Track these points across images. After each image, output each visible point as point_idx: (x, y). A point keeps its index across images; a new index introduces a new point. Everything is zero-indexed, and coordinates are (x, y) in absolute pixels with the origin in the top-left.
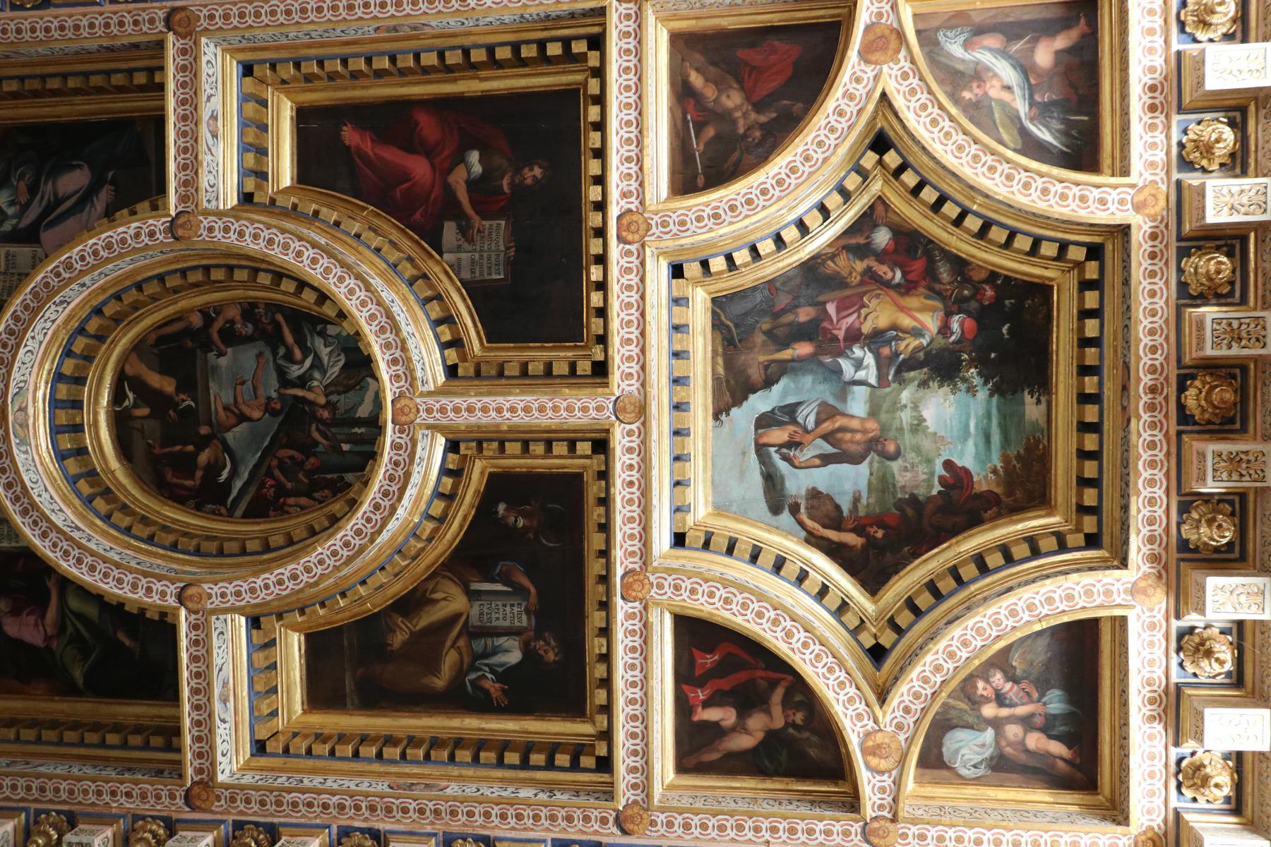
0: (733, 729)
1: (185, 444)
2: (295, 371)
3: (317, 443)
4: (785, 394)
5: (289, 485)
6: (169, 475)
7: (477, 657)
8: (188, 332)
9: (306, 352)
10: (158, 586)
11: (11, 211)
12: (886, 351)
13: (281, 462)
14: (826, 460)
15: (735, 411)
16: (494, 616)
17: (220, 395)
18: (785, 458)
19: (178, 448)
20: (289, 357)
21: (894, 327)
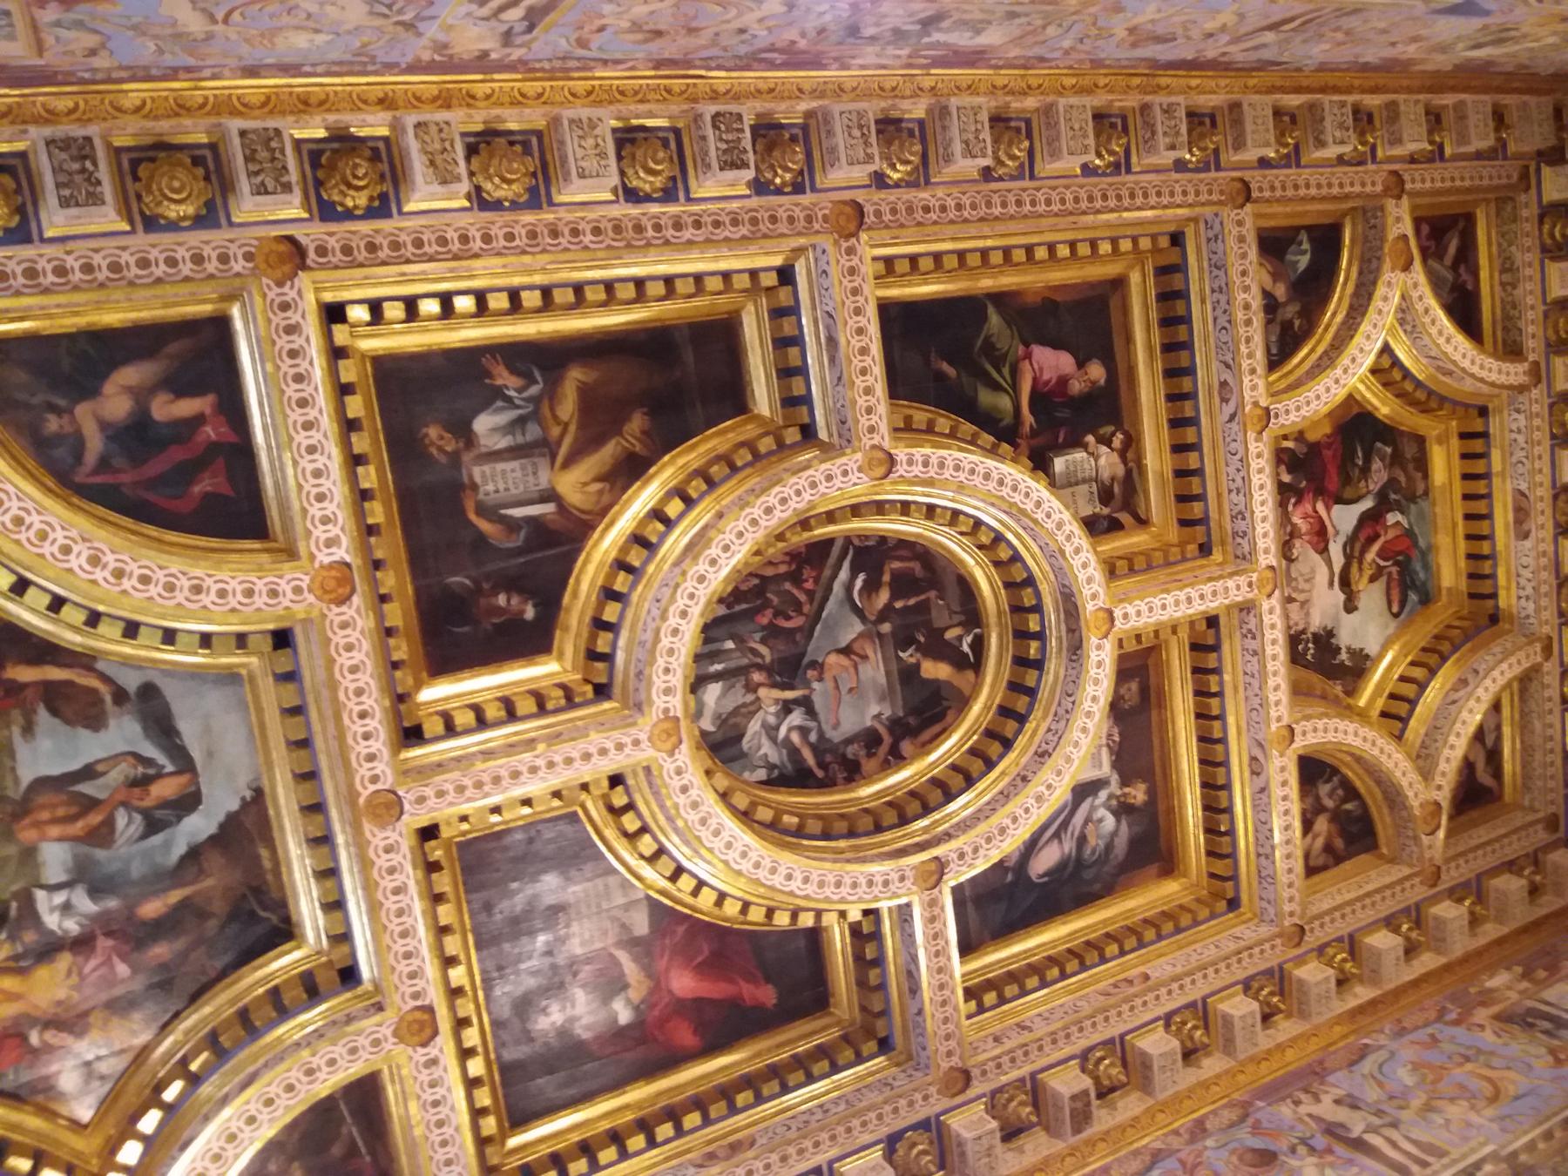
0: (153, 389)
1: (906, 608)
2: (796, 718)
3: (763, 641)
4: (167, 845)
5: (787, 586)
6: (916, 567)
7: (535, 416)
8: (913, 732)
9: (787, 741)
10: (917, 470)
11: (1102, 812)
13: (799, 610)
14: (89, 772)
16: (518, 474)
17: (875, 670)
18: (148, 762)
19: (912, 602)
20: (804, 731)
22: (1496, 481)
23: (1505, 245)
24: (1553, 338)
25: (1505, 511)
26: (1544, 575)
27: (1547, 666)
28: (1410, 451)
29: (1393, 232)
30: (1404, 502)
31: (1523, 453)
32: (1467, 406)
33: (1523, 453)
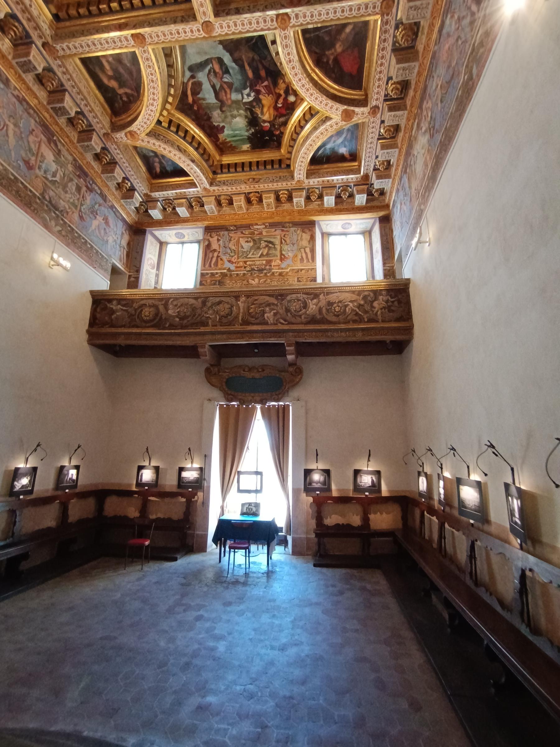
4: (233, 68)
12: (255, 104)
14: (213, 87)
15: (221, 47)
18: (210, 71)
21: (263, 106)
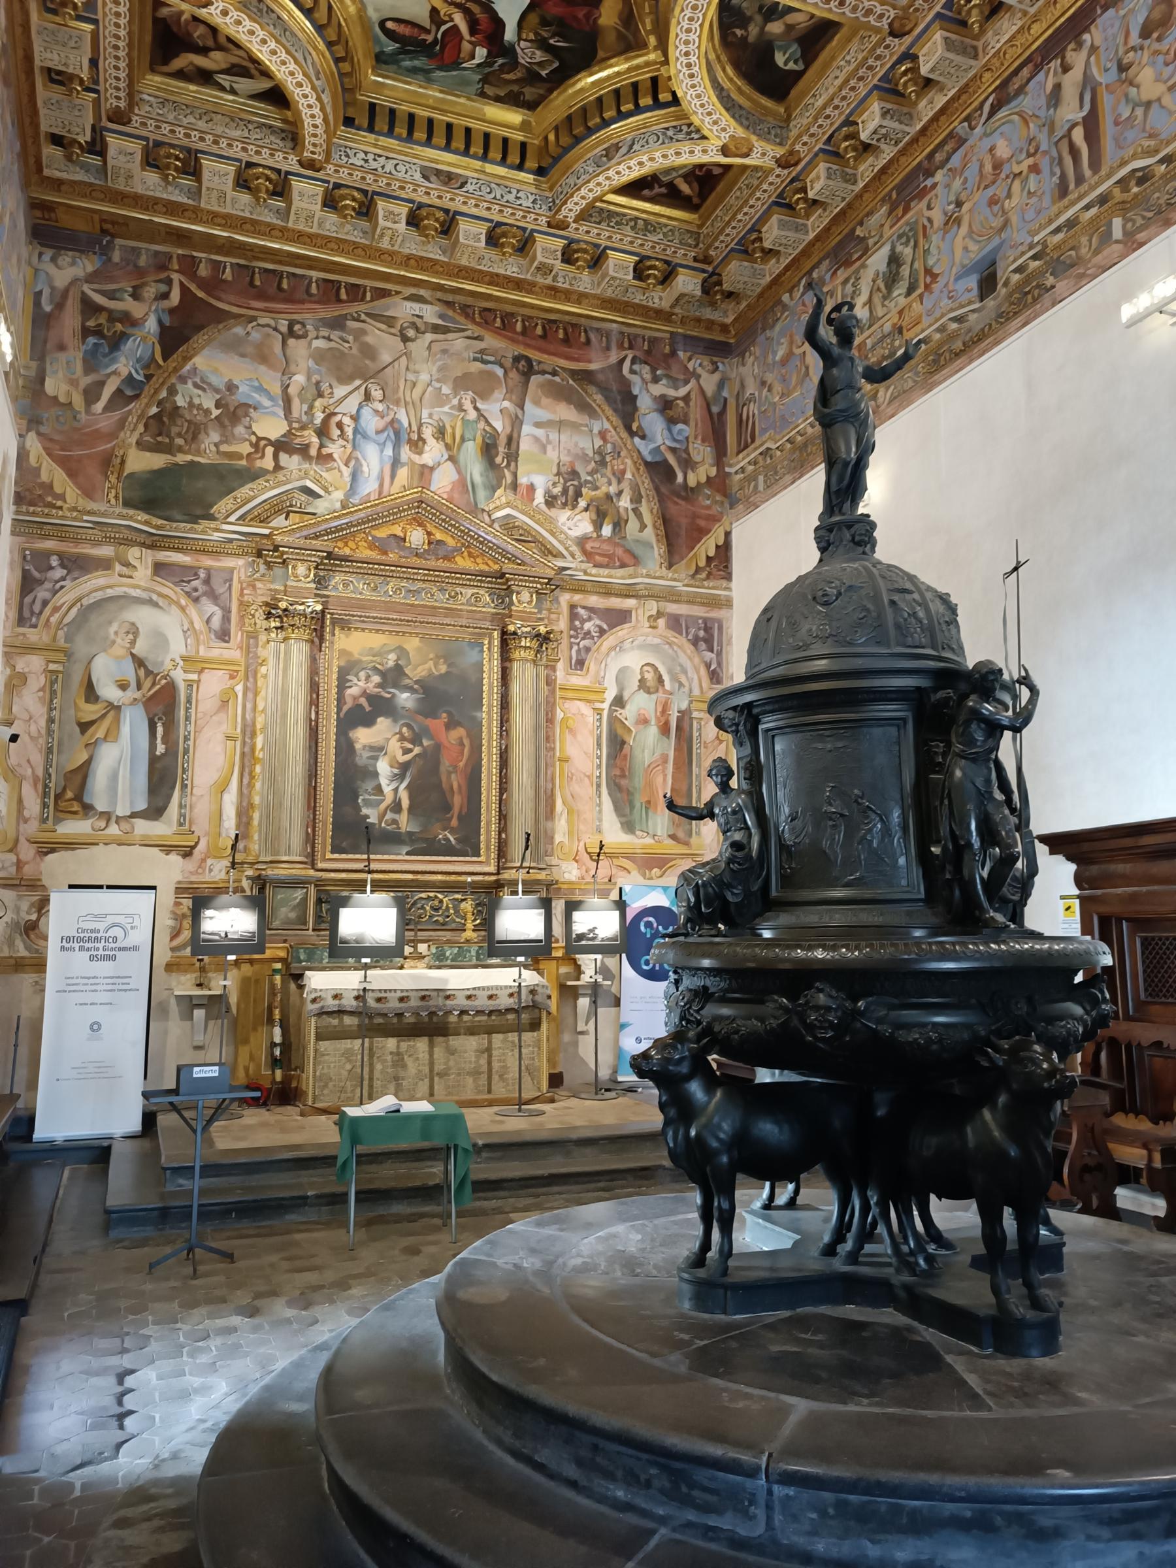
22: (477, 164)
23: (665, 230)
24: (574, 246)
25: (449, 164)
26: (383, 182)
27: (293, 159)
28: (530, 93)
29: (759, 145)
30: (488, 70)
31: (498, 197)
32: (556, 160)
33: (498, 197)
